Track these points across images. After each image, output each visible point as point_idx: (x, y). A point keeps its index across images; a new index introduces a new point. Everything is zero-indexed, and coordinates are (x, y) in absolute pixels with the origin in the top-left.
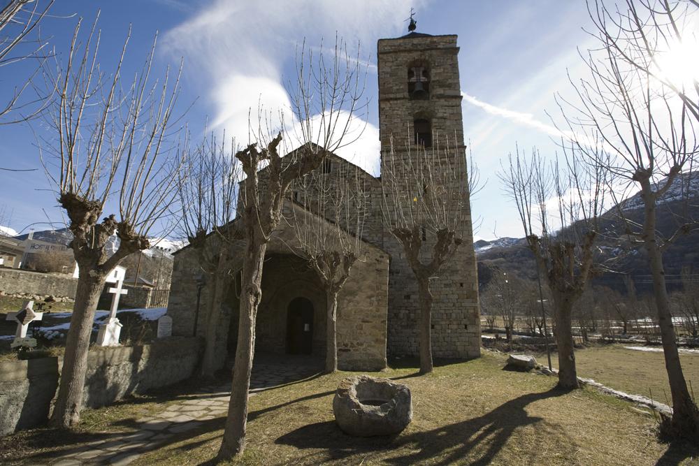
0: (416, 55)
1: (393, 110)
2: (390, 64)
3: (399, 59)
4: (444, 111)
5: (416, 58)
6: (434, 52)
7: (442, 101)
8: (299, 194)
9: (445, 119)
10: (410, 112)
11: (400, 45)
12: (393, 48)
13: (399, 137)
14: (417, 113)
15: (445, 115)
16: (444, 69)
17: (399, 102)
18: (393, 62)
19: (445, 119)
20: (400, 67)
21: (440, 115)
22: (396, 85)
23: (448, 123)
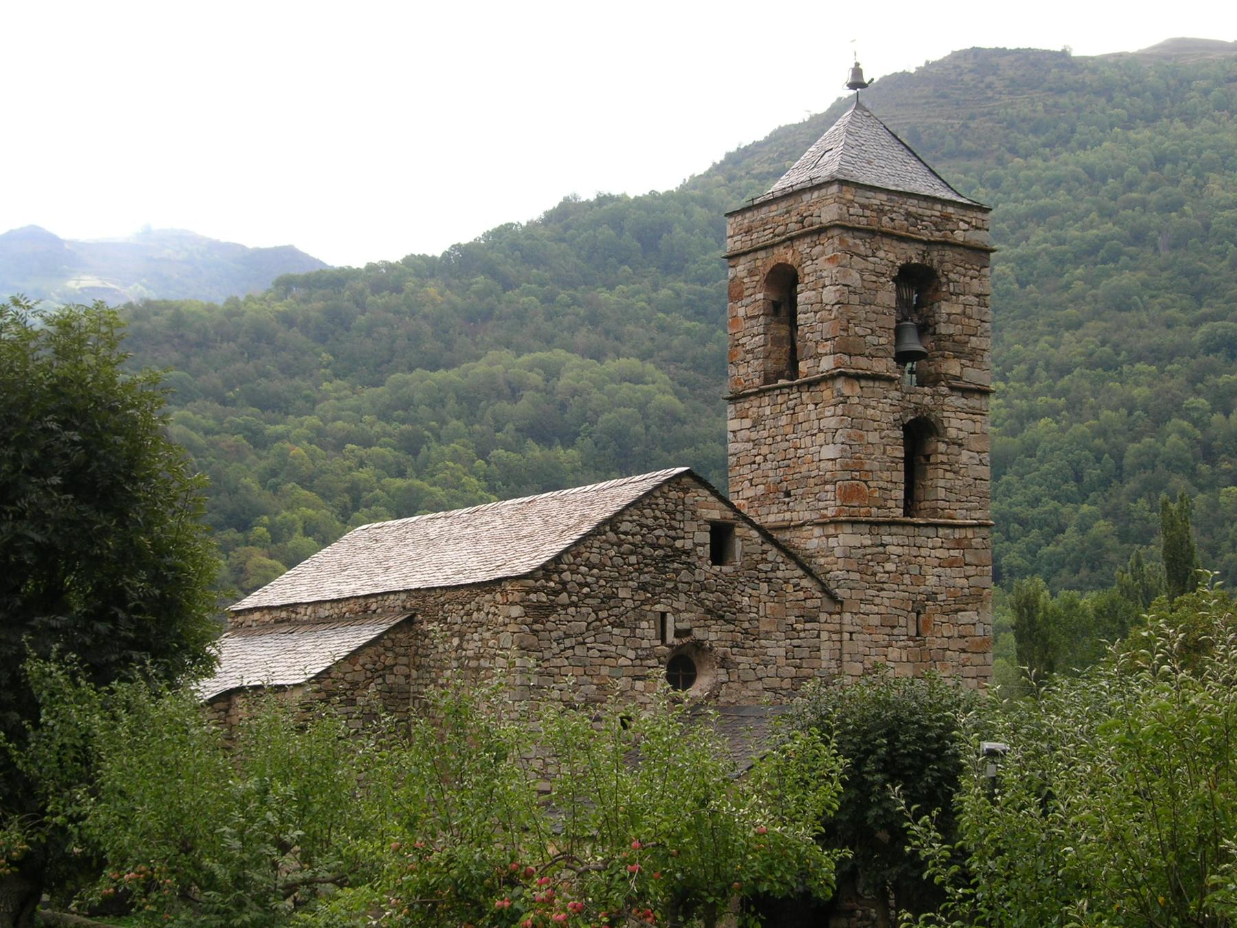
0: (913, 254)
1: (866, 407)
2: (861, 264)
3: (881, 254)
4: (955, 422)
5: (915, 261)
6: (949, 254)
7: (956, 400)
8: (670, 618)
9: (960, 445)
10: (897, 416)
11: (881, 211)
12: (868, 213)
13: (875, 484)
14: (911, 420)
15: (961, 435)
16: (965, 305)
17: (877, 384)
18: (865, 257)
19: (960, 445)
20: (883, 280)
21: (952, 433)
22: (873, 332)
23: (965, 456)
